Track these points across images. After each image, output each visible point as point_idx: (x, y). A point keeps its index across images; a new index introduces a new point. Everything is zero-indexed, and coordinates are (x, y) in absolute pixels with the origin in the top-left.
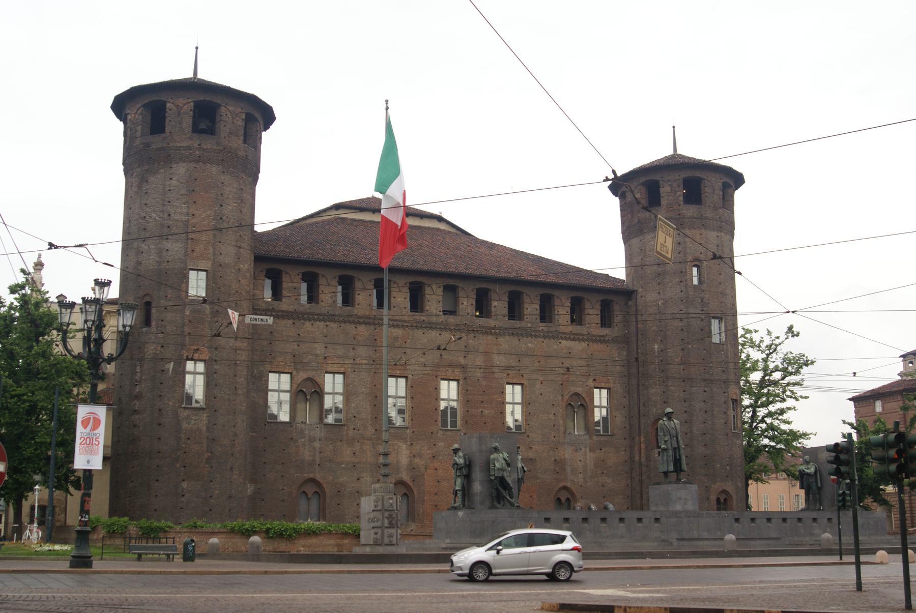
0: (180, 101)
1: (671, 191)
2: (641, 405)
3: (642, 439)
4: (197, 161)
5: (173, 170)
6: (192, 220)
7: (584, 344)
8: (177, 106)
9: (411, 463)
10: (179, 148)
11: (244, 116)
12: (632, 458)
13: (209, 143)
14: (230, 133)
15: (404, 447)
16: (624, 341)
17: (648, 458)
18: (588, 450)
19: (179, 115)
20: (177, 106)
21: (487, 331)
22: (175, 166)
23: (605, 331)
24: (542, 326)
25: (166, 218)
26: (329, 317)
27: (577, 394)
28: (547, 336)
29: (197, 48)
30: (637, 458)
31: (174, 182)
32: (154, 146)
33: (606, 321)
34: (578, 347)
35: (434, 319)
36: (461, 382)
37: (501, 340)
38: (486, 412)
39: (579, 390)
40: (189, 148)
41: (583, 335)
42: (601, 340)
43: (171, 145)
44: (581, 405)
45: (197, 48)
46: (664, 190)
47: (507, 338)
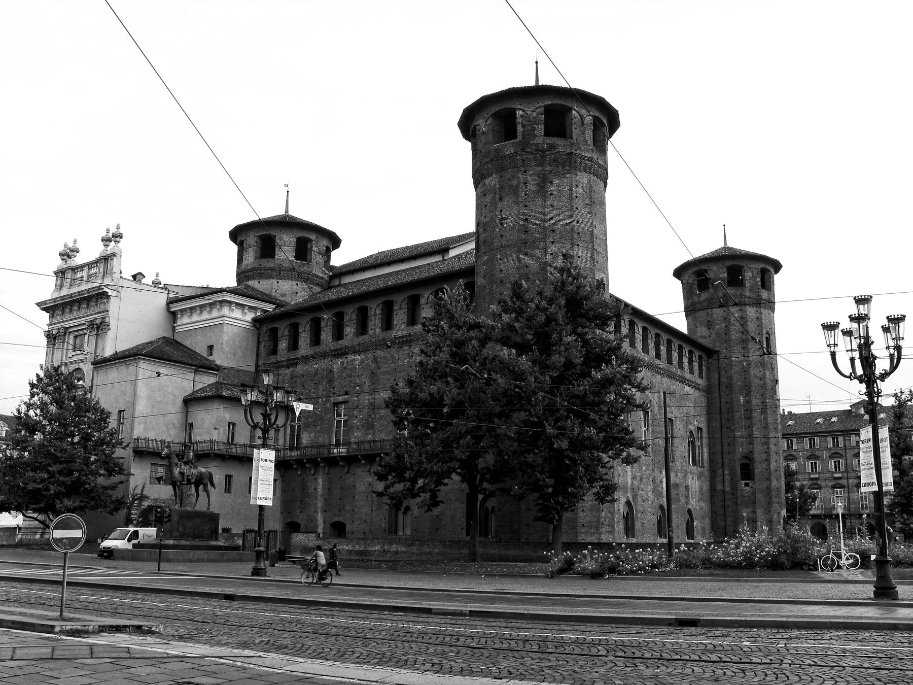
0: (584, 112)
1: (750, 275)
2: (725, 445)
3: (726, 472)
4: (594, 174)
5: (578, 178)
6: (595, 231)
8: (581, 116)
9: (632, 484)
10: (583, 158)
12: (713, 488)
17: (734, 488)
19: (583, 124)
20: (581, 116)
23: (700, 381)
25: (576, 224)
27: (691, 432)
29: (537, 63)
30: (719, 487)
31: (580, 190)
32: (560, 149)
39: (692, 428)
40: (591, 160)
42: (696, 387)
43: (578, 152)
45: (537, 63)
46: (748, 274)
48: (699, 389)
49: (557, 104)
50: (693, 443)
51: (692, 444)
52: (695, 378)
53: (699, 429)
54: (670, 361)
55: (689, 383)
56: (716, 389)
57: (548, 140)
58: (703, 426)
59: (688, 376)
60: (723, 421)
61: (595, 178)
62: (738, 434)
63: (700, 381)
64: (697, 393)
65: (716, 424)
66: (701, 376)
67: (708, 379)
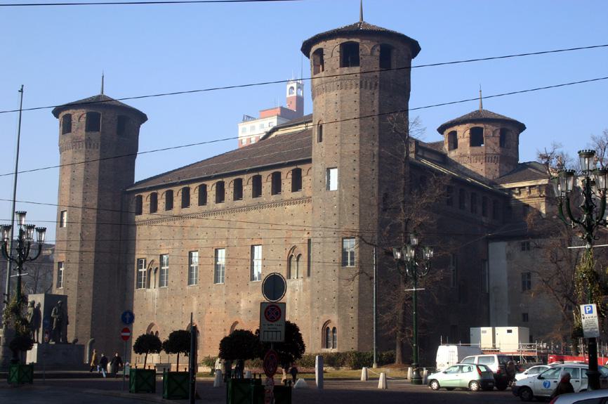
7: (302, 205)
9: (198, 309)
11: (85, 116)
13: (68, 137)
14: (78, 128)
15: (195, 299)
18: (302, 290)
21: (240, 209)
24: (274, 198)
26: (162, 219)
28: (275, 204)
33: (297, 185)
35: (211, 208)
37: (249, 213)
41: (300, 199)
44: (300, 255)
45: (103, 77)
47: (253, 211)
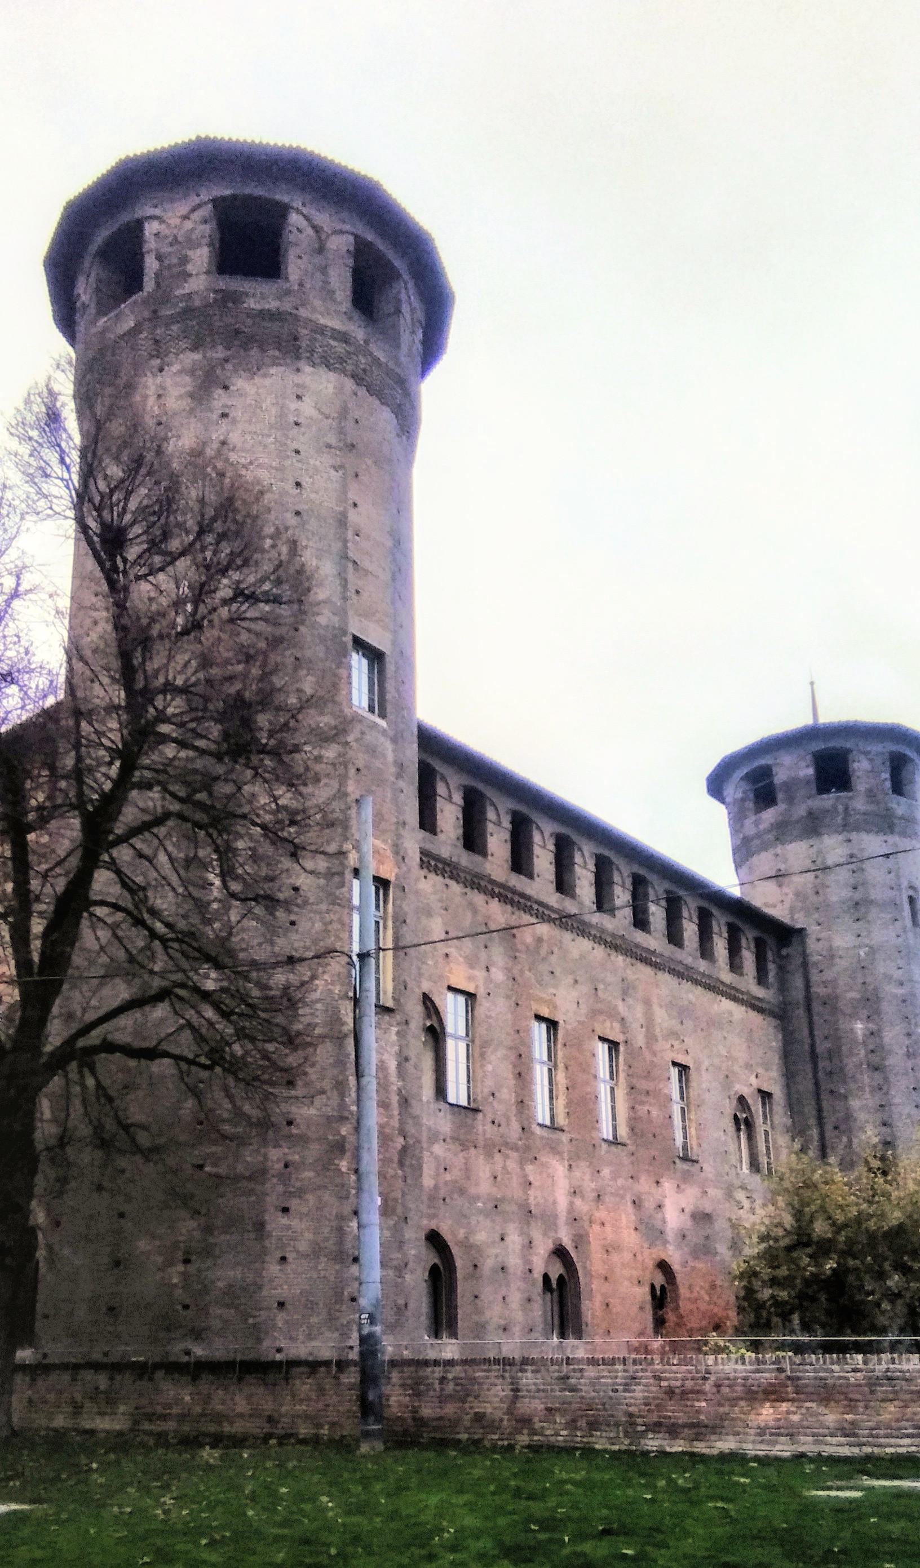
16: (780, 1015)
22: (308, 369)
23: (759, 992)
27: (742, 1099)
34: (738, 1011)
36: (622, 1048)
38: (654, 1113)
39: (746, 1091)
41: (742, 993)
42: (754, 1005)
48: (760, 1010)
49: (249, 198)
50: (749, 1124)
51: (743, 1123)
52: (748, 983)
53: (765, 1096)
54: (674, 937)
55: (733, 994)
56: (801, 1012)
57: (224, 283)
58: (777, 1090)
59: (726, 976)
60: (821, 1075)
61: (362, 392)
62: (855, 1103)
63: (759, 992)
64: (753, 1014)
65: (805, 1085)
66: (761, 978)
67: (783, 986)
